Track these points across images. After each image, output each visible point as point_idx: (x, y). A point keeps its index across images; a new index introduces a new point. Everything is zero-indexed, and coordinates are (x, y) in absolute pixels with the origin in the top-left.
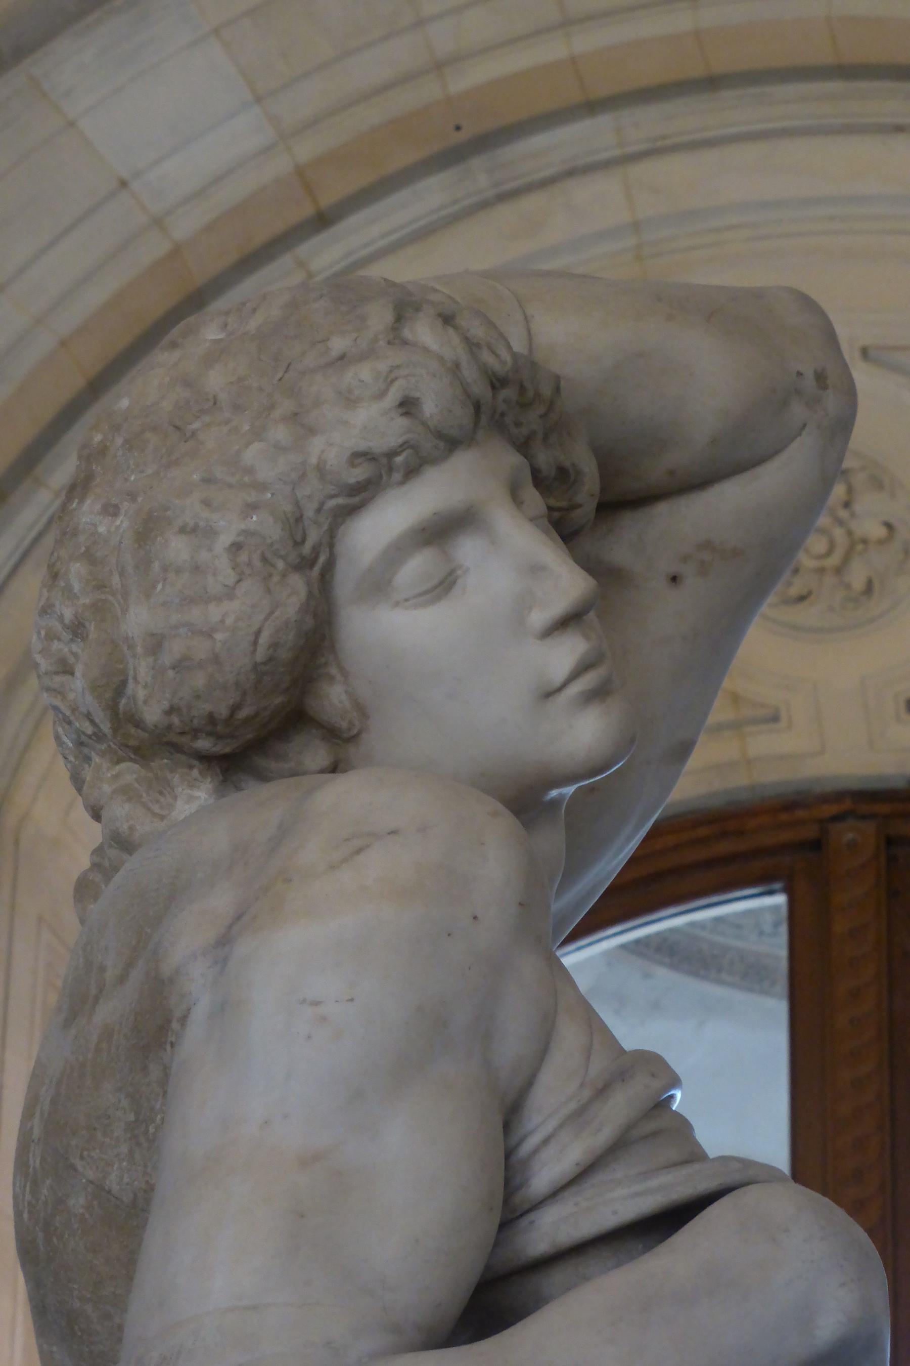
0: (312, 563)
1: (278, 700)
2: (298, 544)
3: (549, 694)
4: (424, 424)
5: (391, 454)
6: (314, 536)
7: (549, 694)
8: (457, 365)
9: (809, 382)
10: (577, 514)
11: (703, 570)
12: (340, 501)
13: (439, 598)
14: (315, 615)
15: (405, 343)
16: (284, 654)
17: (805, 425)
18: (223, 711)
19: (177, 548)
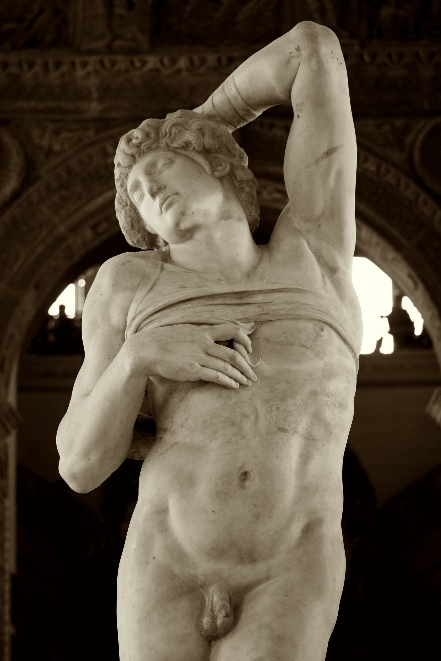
0: (127, 205)
1: (139, 236)
2: (120, 204)
3: (162, 213)
4: (122, 167)
5: (120, 177)
6: (124, 200)
8: (124, 150)
9: (295, 53)
10: (197, 148)
11: (301, 112)
12: (122, 190)
13: (142, 202)
14: (130, 216)
16: (128, 229)
17: (300, 63)
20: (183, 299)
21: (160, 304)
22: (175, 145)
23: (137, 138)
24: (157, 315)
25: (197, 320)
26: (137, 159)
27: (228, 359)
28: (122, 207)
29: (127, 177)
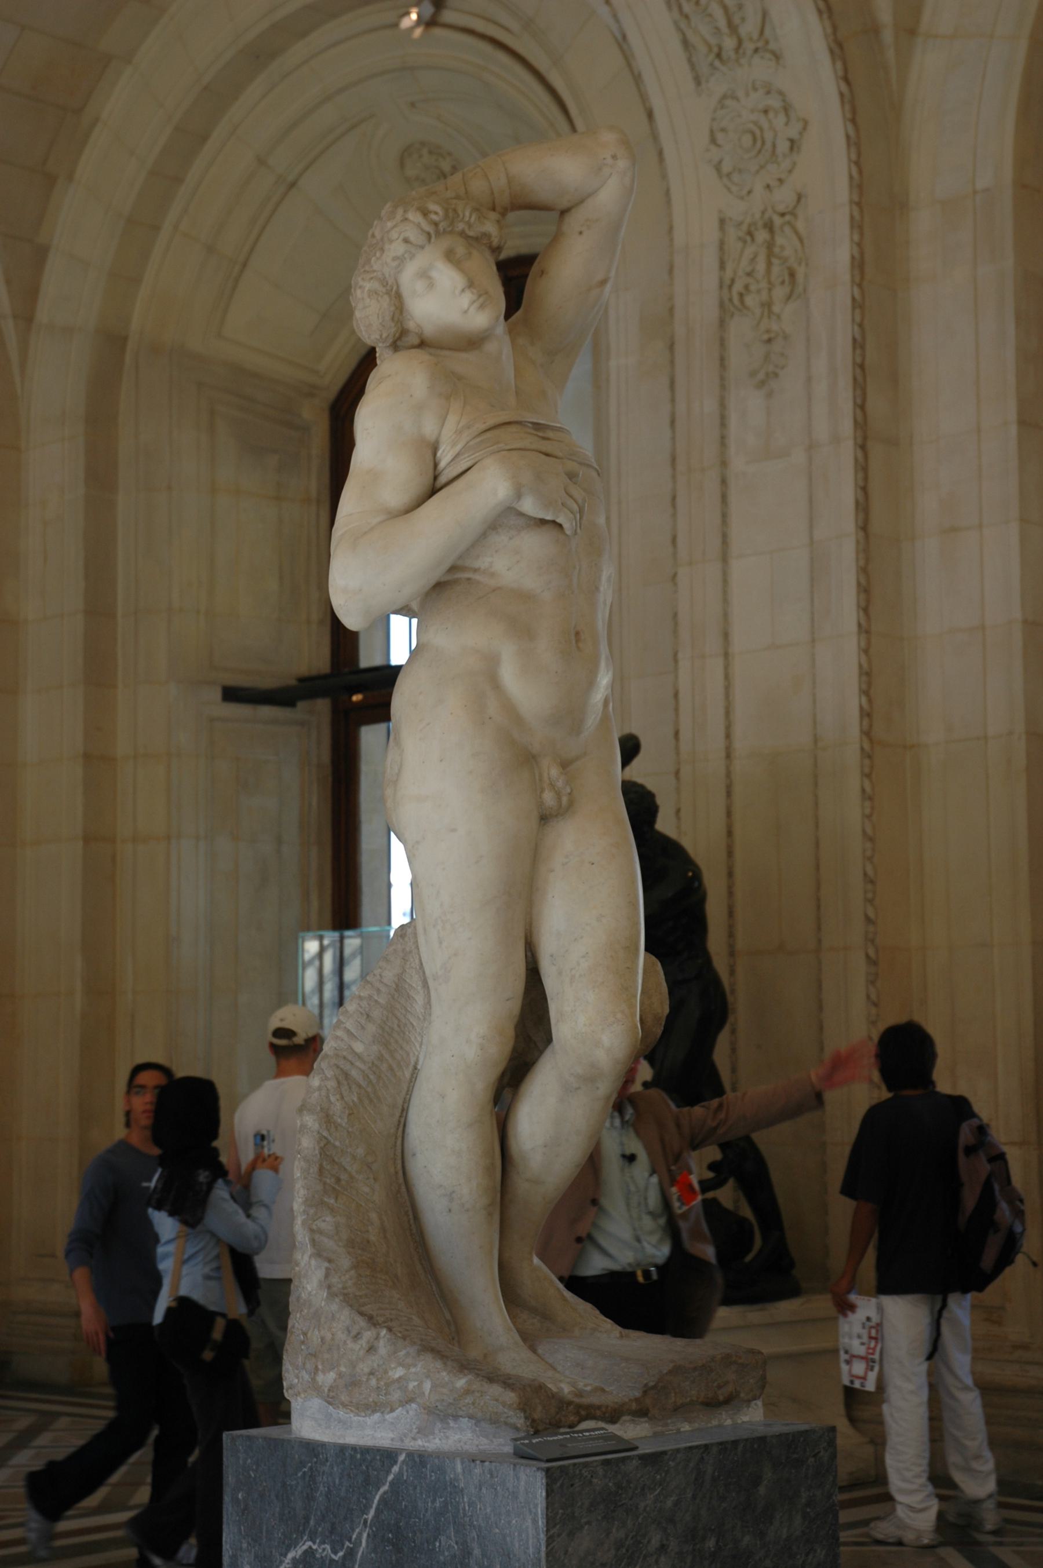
1: (393, 330)
7: (466, 312)
9: (609, 161)
15: (406, 219)
18: (378, 337)
19: (359, 292)
20: (508, 420)
21: (491, 422)
22: (471, 234)
23: (436, 213)
24: (488, 435)
25: (544, 449)
26: (433, 240)
27: (580, 502)
28: (384, 290)
29: (412, 256)
